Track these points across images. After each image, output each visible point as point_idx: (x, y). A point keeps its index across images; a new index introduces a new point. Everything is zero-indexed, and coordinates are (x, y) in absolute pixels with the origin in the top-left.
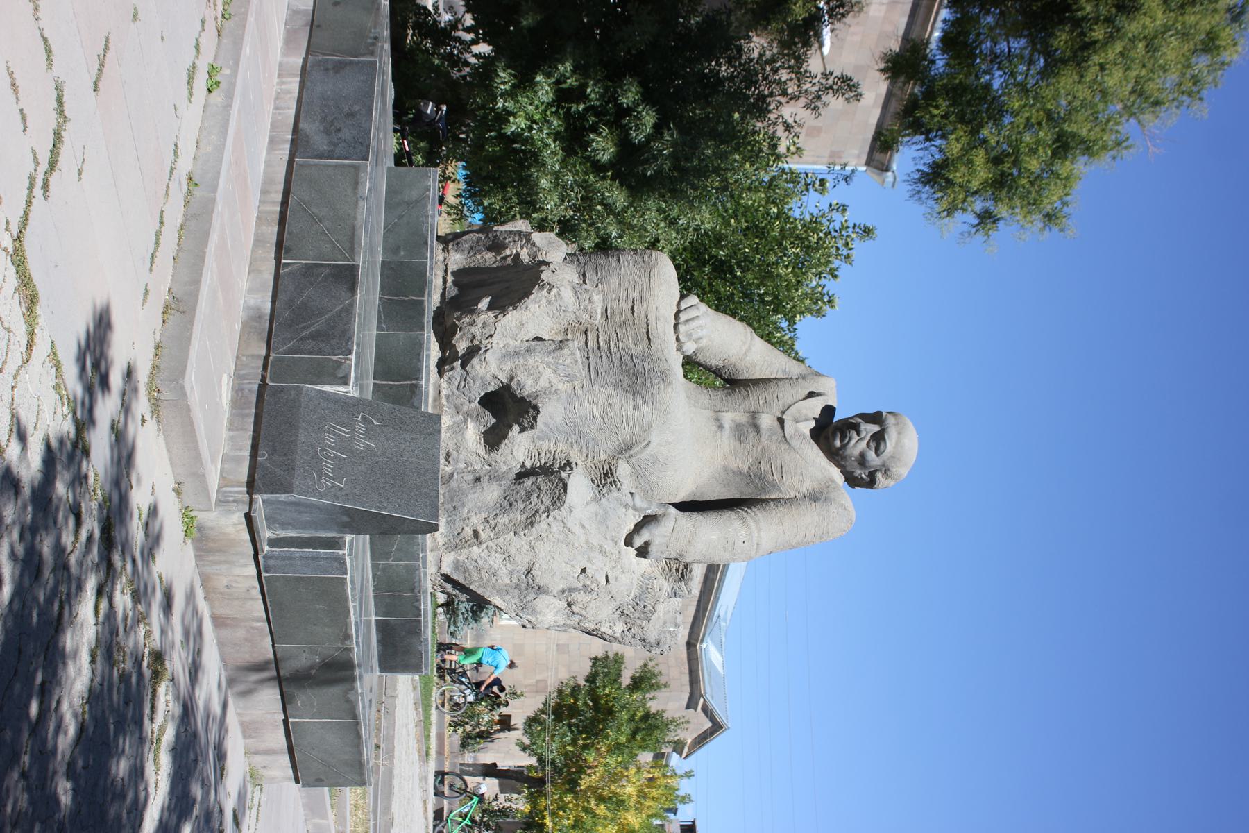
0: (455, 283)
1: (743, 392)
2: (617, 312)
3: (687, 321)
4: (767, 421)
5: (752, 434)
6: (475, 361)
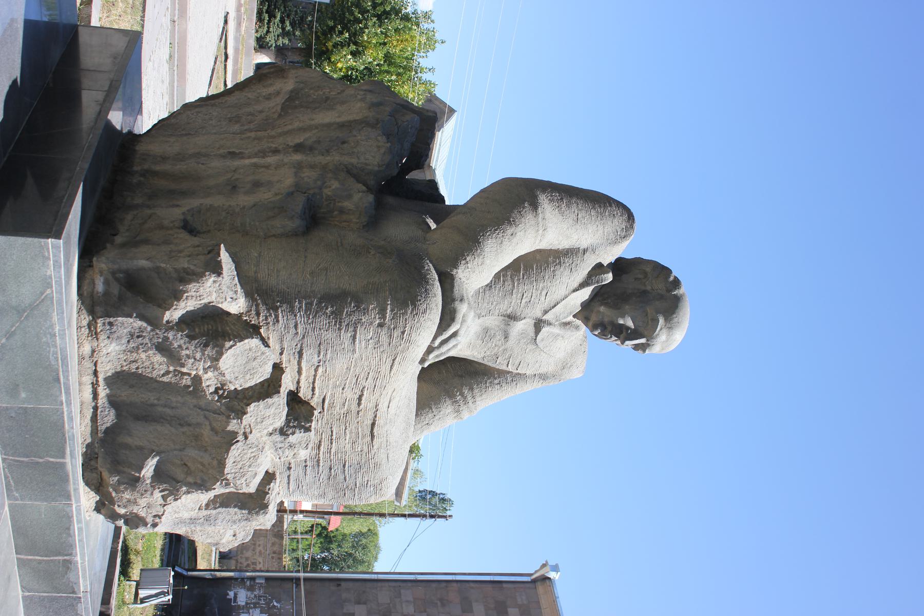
0: (113, 402)
1: (509, 283)
2: (338, 402)
5: (499, 336)
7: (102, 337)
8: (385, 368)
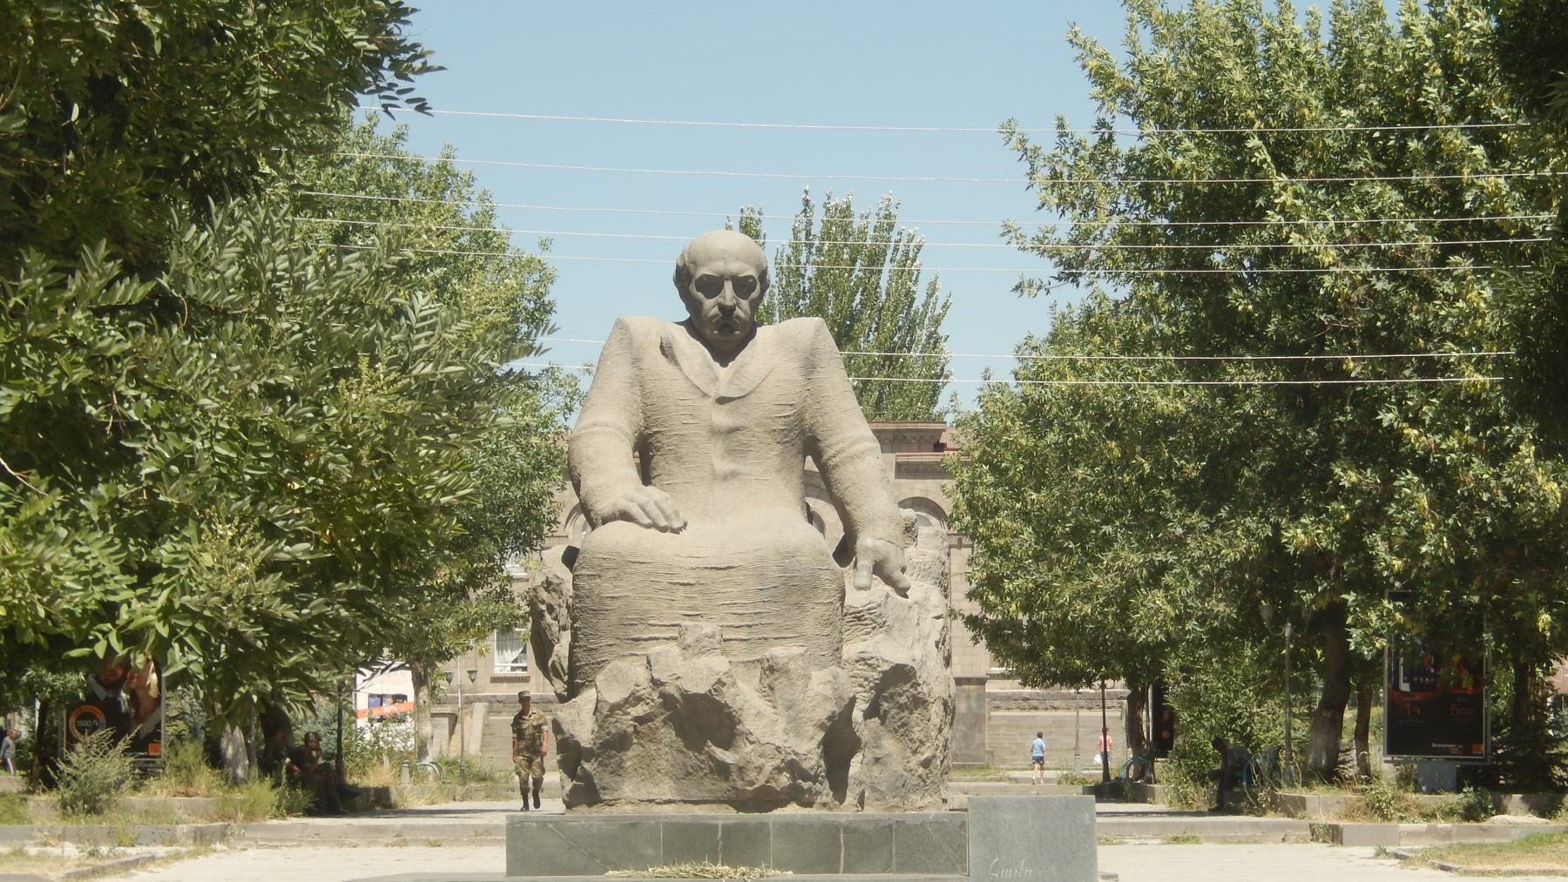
3: (667, 518)
4: (722, 418)
5: (739, 436)
6: (806, 765)
7: (616, 795)
8: (643, 568)
